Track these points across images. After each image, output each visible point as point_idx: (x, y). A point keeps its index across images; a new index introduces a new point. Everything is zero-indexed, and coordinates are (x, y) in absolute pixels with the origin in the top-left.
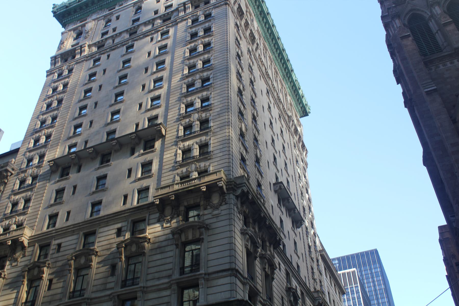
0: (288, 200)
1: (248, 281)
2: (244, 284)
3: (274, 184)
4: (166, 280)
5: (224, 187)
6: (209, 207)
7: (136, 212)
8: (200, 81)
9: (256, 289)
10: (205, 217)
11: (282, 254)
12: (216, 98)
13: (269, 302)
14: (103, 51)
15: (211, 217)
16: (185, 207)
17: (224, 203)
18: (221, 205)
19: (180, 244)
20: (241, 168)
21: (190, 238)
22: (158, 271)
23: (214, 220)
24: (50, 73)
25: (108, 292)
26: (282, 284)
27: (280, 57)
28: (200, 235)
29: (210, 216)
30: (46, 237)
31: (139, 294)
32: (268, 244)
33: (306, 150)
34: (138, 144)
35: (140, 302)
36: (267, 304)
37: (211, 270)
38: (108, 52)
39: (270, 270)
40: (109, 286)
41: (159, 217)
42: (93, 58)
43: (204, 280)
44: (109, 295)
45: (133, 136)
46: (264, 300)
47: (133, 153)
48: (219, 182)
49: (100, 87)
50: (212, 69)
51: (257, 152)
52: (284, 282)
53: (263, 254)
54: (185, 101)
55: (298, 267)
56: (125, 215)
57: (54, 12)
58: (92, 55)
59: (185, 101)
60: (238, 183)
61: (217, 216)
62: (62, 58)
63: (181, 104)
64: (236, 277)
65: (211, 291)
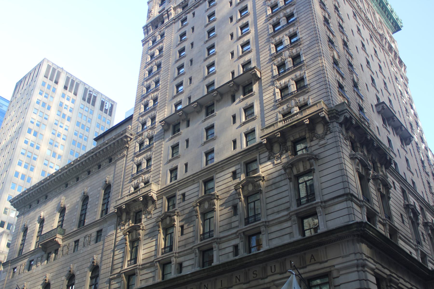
0: (393, 119)
1: (364, 203)
2: (361, 207)
3: (376, 106)
4: (285, 213)
5: (327, 117)
6: (314, 139)
7: (246, 154)
8: (285, 18)
9: (373, 210)
10: (313, 149)
11: (395, 173)
12: (303, 32)
13: (389, 221)
14: (188, 10)
15: (319, 147)
16: (292, 141)
17: (328, 132)
18: (326, 135)
19: (293, 177)
20: (340, 96)
21: (302, 170)
22: (276, 205)
23: (322, 150)
24: (145, 42)
25: (234, 231)
28: (311, 166)
29: (317, 147)
30: (171, 189)
31: (262, 229)
32: (379, 165)
33: (405, 65)
34: (237, 91)
35: (265, 235)
36: (387, 223)
37: (326, 198)
38: (192, 10)
39: (385, 190)
40: (234, 225)
41: (269, 155)
42: (180, 19)
43: (322, 208)
44: (236, 233)
45: (231, 84)
46: (383, 219)
47: (234, 100)
48: (320, 112)
49: (192, 44)
50: (294, 4)
51: (353, 77)
52: (401, 200)
53: (375, 176)
54: (273, 41)
55: (413, 183)
56: (237, 158)
58: (179, 17)
59: (273, 41)
60: (339, 110)
61: (324, 146)
62: (152, 26)
63: (266, 7)
65: (329, 217)
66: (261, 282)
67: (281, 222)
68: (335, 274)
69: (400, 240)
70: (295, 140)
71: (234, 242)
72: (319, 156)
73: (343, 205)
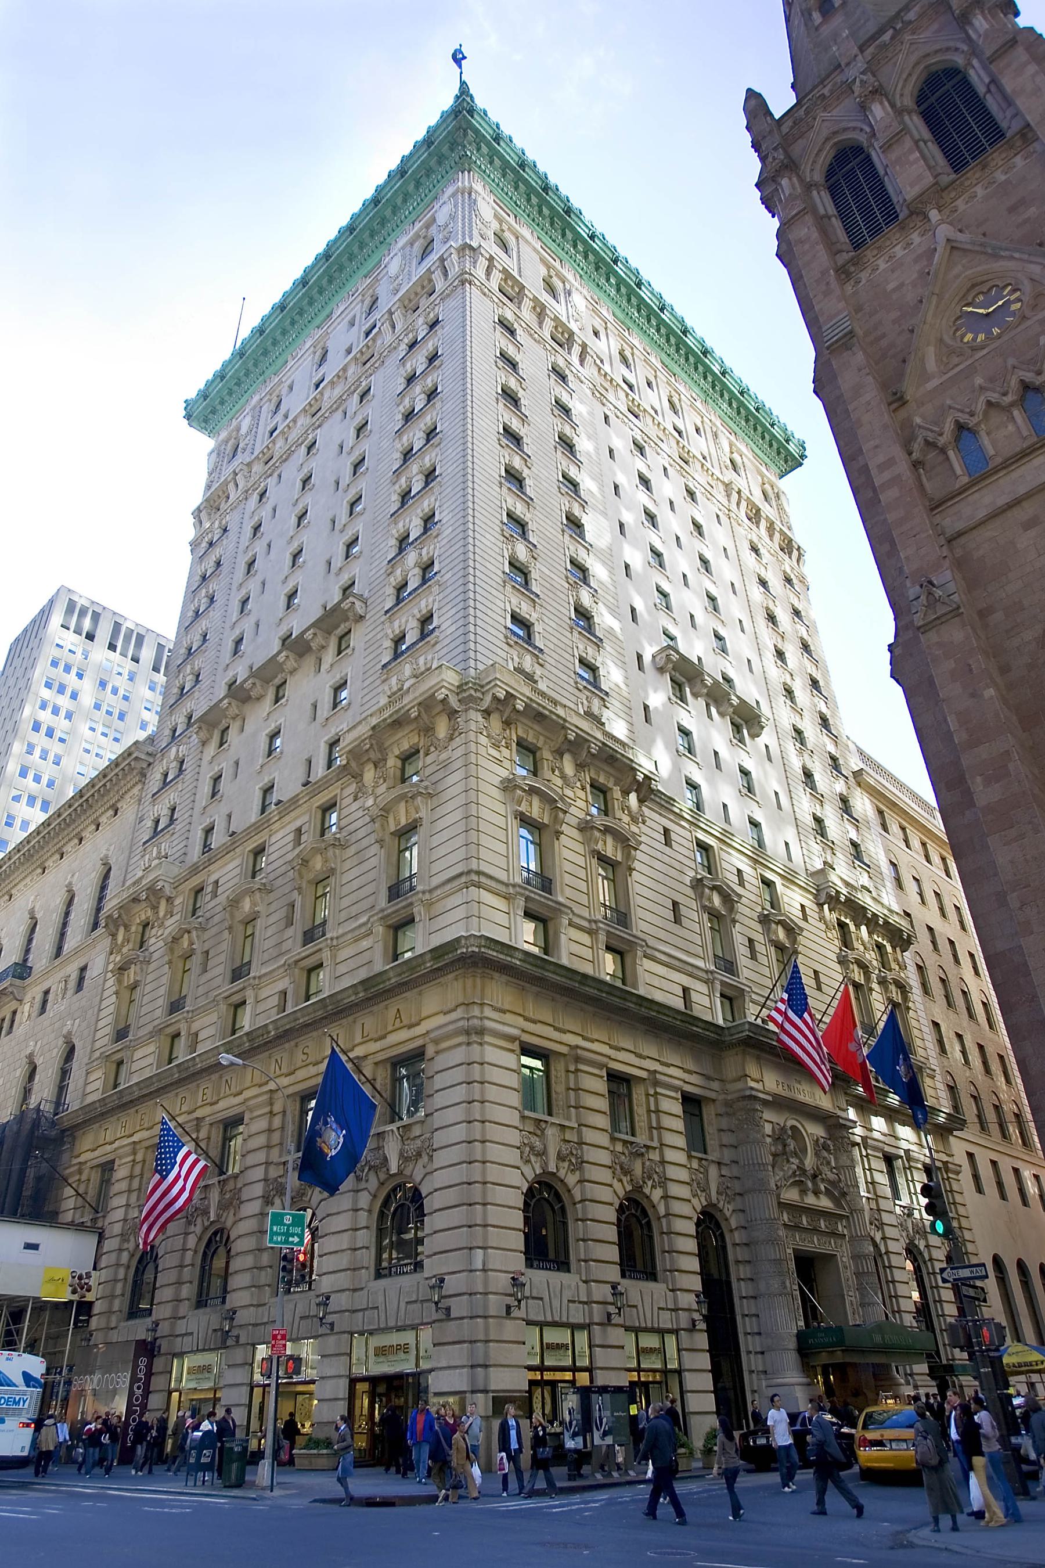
1: (518, 889)
17: (457, 734)
18: (452, 739)
21: (403, 822)
24: (194, 545)
37: (436, 881)
40: (285, 946)
44: (284, 965)
57: (188, 417)
64: (478, 886)
68: (430, 1051)
70: (401, 753)
71: (281, 985)
73: (457, 899)
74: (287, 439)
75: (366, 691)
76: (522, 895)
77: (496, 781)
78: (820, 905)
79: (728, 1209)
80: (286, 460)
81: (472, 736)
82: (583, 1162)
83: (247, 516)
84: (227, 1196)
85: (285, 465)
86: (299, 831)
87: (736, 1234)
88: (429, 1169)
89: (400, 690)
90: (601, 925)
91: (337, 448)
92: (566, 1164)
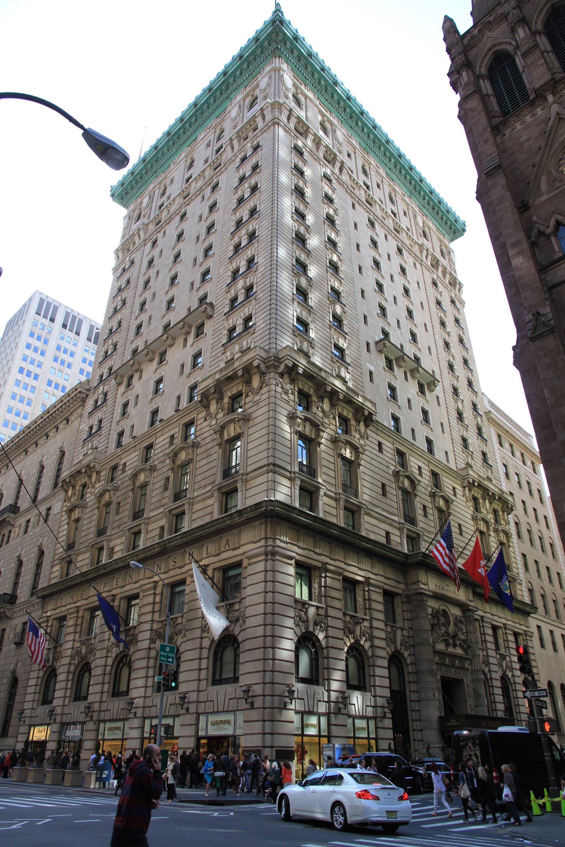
0: (403, 359)
3: (377, 343)
4: (209, 488)
16: (230, 397)
17: (264, 385)
21: (232, 434)
23: (255, 408)
24: (115, 270)
25: (161, 510)
26: (384, 468)
27: (398, 168)
29: (251, 404)
32: (353, 422)
37: (250, 469)
40: (163, 502)
44: (162, 512)
57: (113, 196)
66: (178, 571)
67: (205, 499)
69: (366, 518)
70: (232, 395)
72: (250, 416)
74: (169, 211)
75: (212, 359)
76: (299, 478)
77: (286, 413)
78: (464, 487)
79: (406, 654)
80: (168, 223)
81: (273, 387)
82: (328, 626)
83: (145, 255)
84: (130, 637)
85: (168, 226)
86: (172, 437)
87: (410, 667)
88: (243, 627)
89: (233, 359)
90: (342, 496)
91: (197, 218)
92: (319, 627)
